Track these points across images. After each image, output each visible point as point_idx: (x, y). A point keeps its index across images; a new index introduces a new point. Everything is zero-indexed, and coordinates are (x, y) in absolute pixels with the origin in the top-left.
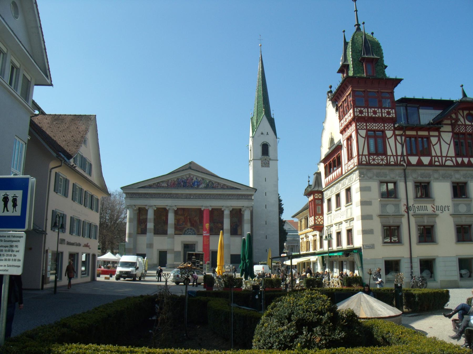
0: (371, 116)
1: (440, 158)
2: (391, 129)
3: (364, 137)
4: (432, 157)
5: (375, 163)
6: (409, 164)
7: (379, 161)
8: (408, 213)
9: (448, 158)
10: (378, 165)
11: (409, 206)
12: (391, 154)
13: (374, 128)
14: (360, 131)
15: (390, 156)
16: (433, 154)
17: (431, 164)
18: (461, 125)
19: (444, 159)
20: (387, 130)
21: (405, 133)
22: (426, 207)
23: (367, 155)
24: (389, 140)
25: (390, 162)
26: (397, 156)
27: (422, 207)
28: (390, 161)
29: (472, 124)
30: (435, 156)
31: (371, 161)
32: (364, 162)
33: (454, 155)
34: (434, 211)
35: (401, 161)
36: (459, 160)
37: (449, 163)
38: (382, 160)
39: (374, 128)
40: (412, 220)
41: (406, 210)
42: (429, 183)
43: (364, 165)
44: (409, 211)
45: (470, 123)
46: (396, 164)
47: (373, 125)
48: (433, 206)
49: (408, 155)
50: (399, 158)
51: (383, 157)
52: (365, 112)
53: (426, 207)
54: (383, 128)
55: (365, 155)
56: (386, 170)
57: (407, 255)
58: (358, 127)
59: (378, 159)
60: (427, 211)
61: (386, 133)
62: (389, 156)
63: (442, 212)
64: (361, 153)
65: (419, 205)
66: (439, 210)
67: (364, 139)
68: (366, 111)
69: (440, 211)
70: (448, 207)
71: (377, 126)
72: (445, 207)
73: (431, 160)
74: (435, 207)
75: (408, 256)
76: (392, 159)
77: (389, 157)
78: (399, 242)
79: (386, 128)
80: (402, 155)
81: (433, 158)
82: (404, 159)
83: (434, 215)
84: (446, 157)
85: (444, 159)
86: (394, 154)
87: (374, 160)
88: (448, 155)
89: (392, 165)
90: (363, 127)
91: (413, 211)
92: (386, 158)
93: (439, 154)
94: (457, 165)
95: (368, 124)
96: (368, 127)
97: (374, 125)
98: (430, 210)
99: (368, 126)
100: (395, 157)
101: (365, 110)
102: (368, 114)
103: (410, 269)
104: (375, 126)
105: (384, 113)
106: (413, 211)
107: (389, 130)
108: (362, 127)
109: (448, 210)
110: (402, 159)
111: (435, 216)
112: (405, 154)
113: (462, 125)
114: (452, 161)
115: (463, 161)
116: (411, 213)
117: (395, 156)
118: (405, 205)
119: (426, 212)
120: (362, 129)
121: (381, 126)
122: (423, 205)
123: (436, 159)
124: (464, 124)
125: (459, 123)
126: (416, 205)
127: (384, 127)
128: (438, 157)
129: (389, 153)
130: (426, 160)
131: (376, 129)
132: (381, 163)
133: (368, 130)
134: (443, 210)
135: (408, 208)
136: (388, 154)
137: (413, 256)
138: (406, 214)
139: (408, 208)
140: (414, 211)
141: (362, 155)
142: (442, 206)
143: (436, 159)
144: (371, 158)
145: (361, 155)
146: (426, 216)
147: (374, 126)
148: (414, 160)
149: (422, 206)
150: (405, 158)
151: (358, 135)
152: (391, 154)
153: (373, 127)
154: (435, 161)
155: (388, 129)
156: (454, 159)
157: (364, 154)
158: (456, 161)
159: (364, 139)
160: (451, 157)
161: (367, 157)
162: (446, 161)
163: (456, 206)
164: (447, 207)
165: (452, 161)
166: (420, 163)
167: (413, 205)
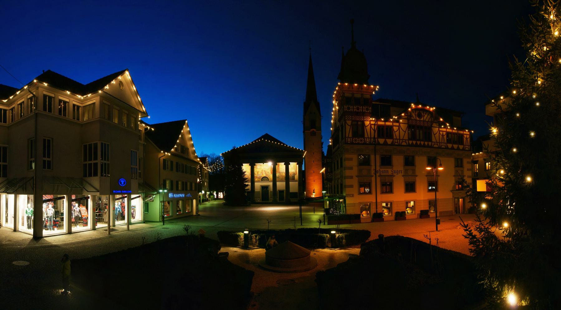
1: (398, 140)
3: (350, 125)
6: (379, 144)
7: (359, 141)
8: (376, 175)
9: (403, 141)
10: (358, 144)
15: (366, 138)
16: (395, 137)
17: (392, 144)
18: (413, 120)
19: (401, 141)
20: (365, 121)
21: (377, 123)
23: (351, 137)
25: (366, 142)
26: (371, 138)
30: (395, 139)
31: (354, 141)
32: (349, 142)
33: (407, 139)
35: (373, 142)
36: (410, 142)
37: (404, 144)
39: (357, 119)
43: (349, 144)
45: (419, 119)
46: (370, 144)
49: (377, 138)
50: (372, 139)
51: (362, 139)
54: (363, 119)
55: (350, 138)
58: (346, 119)
62: (366, 138)
64: (347, 136)
65: (383, 170)
67: (350, 127)
68: (352, 108)
73: (393, 142)
74: (393, 171)
75: (375, 201)
76: (368, 140)
77: (365, 139)
78: (370, 192)
79: (365, 119)
81: (394, 140)
82: (375, 140)
83: (392, 176)
84: (403, 140)
85: (401, 141)
86: (369, 137)
87: (356, 140)
88: (404, 139)
89: (368, 144)
93: (398, 138)
94: (409, 145)
97: (357, 117)
98: (390, 173)
100: (370, 139)
101: (352, 107)
103: (376, 209)
105: (364, 109)
109: (401, 173)
110: (374, 140)
112: (376, 137)
113: (414, 120)
114: (406, 142)
115: (412, 143)
116: (378, 174)
119: (388, 174)
120: (349, 120)
123: (396, 141)
124: (415, 118)
126: (381, 170)
128: (397, 139)
129: (366, 136)
130: (389, 141)
132: (360, 142)
133: (353, 121)
135: (376, 172)
136: (365, 137)
138: (374, 175)
141: (348, 137)
143: (396, 141)
144: (354, 140)
148: (381, 141)
150: (376, 139)
151: (346, 124)
153: (356, 119)
156: (407, 141)
157: (349, 137)
158: (408, 142)
159: (350, 127)
160: (406, 140)
162: (402, 142)
165: (406, 142)
166: (385, 144)
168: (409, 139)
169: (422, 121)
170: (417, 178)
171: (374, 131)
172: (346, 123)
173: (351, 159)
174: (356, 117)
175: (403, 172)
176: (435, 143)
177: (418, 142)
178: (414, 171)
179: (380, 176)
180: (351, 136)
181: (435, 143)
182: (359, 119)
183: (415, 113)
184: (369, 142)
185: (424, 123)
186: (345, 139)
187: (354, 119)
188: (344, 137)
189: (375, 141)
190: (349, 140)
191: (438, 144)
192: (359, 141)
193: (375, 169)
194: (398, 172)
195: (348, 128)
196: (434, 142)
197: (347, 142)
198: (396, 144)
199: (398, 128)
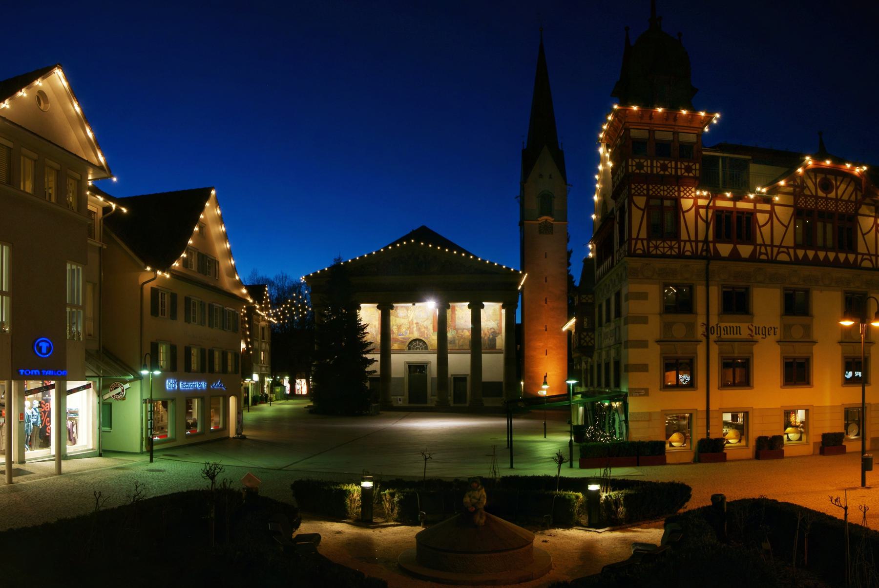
0: (658, 173)
1: (769, 249)
2: (690, 196)
4: (756, 245)
5: (659, 252)
6: (717, 256)
8: (707, 337)
9: (782, 249)
10: (664, 256)
11: (710, 327)
12: (687, 239)
13: (662, 193)
14: (634, 198)
15: (685, 241)
16: (759, 241)
17: (753, 258)
19: (775, 250)
20: (683, 197)
21: (714, 203)
22: (738, 328)
23: (645, 239)
24: (685, 214)
25: (684, 252)
26: (697, 241)
27: (732, 328)
28: (685, 250)
29: (827, 196)
30: (761, 245)
31: (651, 249)
33: (792, 245)
34: (751, 336)
35: (702, 250)
36: (801, 253)
37: (783, 257)
38: (671, 248)
39: (662, 193)
40: (715, 350)
41: (706, 334)
42: (747, 289)
43: (639, 256)
44: (710, 334)
45: (824, 195)
46: (694, 256)
47: (659, 188)
48: (751, 327)
49: (714, 242)
50: (700, 245)
51: (673, 243)
53: (738, 328)
54: (676, 194)
55: (642, 240)
56: (677, 264)
57: (703, 408)
58: (633, 191)
59: (664, 247)
60: (740, 334)
61: (680, 202)
62: (682, 241)
63: (764, 336)
64: (634, 236)
65: (728, 325)
66: (759, 334)
68: (649, 165)
69: (761, 336)
70: (774, 330)
71: (666, 191)
72: (770, 329)
75: (704, 408)
76: (688, 247)
77: (682, 244)
78: (691, 385)
79: (682, 194)
80: (706, 241)
81: (758, 247)
82: (708, 246)
83: (752, 341)
84: (780, 246)
85: (775, 250)
86: (693, 238)
87: (656, 247)
88: (783, 245)
90: (642, 192)
91: (717, 334)
93: (768, 242)
94: (797, 261)
95: (651, 187)
96: (651, 192)
98: (745, 334)
99: (651, 190)
100: (693, 244)
103: (705, 428)
104: (664, 190)
105: (681, 169)
106: (717, 334)
108: (639, 191)
109: (775, 334)
110: (705, 248)
111: (753, 343)
112: (711, 238)
113: (812, 196)
114: (788, 254)
115: (806, 255)
116: (713, 337)
118: (705, 325)
120: (639, 195)
121: (673, 191)
122: (734, 325)
123: (763, 250)
124: (814, 194)
125: (807, 192)
126: (723, 325)
128: (766, 246)
129: (684, 236)
130: (745, 250)
132: (669, 253)
133: (649, 198)
134: (765, 334)
135: (708, 330)
136: (682, 239)
137: (711, 408)
138: (704, 339)
139: (707, 329)
140: (719, 335)
141: (637, 239)
142: (765, 328)
143: (763, 250)
144: (651, 245)
145: (634, 239)
146: (736, 343)
147: (661, 190)
148: (725, 249)
149: (733, 327)
150: (711, 245)
151: (633, 205)
153: (659, 192)
154: (761, 253)
156: (791, 251)
157: (640, 237)
158: (795, 254)
159: (641, 212)
160: (787, 248)
161: (645, 242)
162: (778, 253)
163: (787, 328)
164: (773, 329)
165: (788, 254)
166: (735, 256)
167: (717, 325)
168: (797, 246)
169: (832, 199)
170: (816, 349)
171: (704, 224)
172: (631, 201)
173: (643, 296)
174: (659, 188)
175: (778, 331)
176: (865, 257)
177: (822, 255)
178: (808, 329)
179: (718, 341)
180: (643, 234)
181: (865, 257)
182: (666, 193)
183: (814, 180)
184: (692, 252)
185: (837, 206)
186: (630, 244)
187: (654, 192)
188: (626, 237)
189: (708, 250)
190: (639, 245)
191: (874, 258)
192: (666, 250)
193: (705, 322)
194: (765, 332)
195: (637, 215)
196: (863, 254)
197: (635, 250)
198: (763, 257)
199: (767, 215)
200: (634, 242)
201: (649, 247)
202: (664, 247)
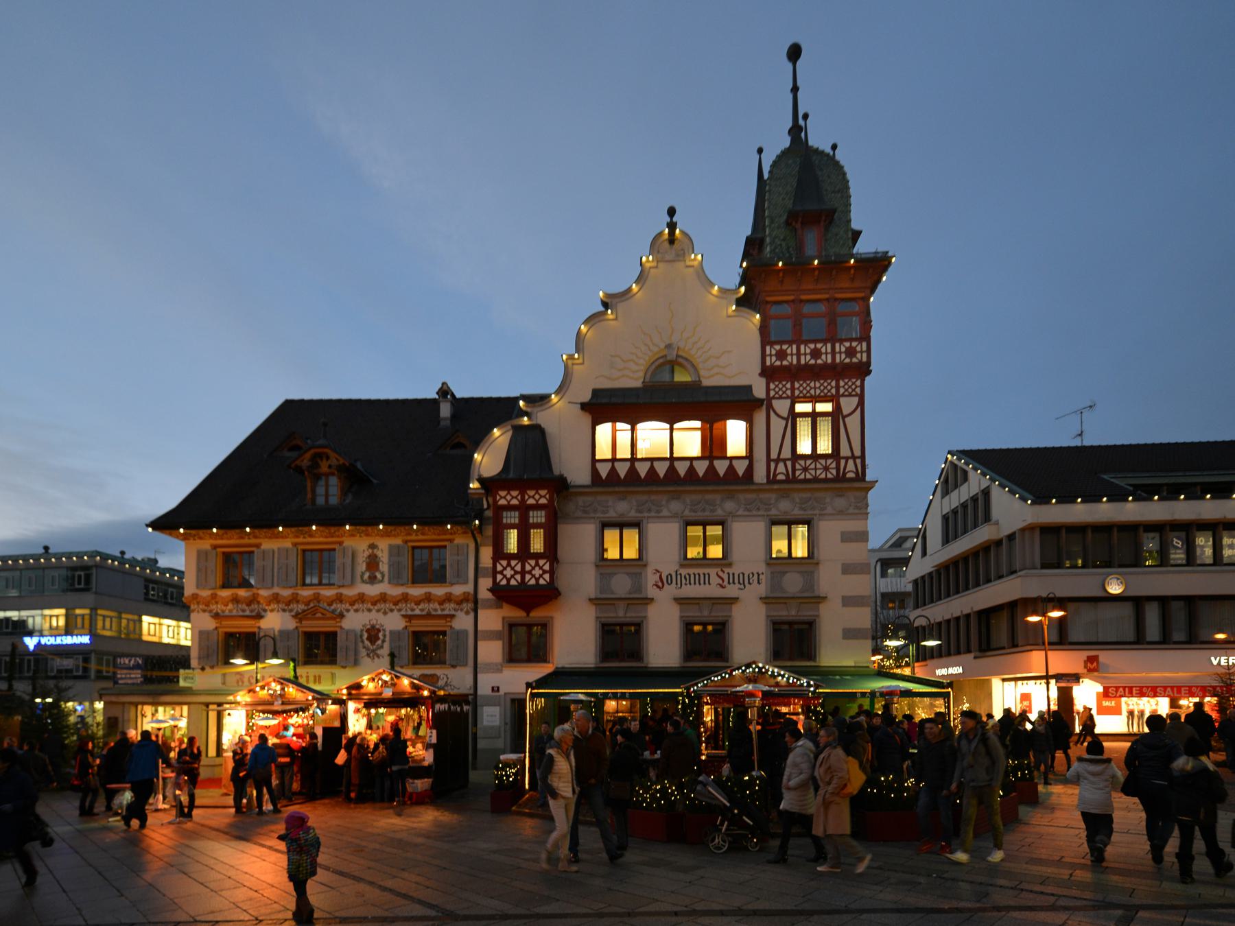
0: (806, 364)
2: (854, 393)
5: (808, 476)
10: (816, 480)
12: (849, 454)
14: (775, 402)
15: (847, 459)
20: (843, 395)
23: (788, 459)
24: (846, 419)
31: (798, 473)
38: (826, 469)
52: (792, 355)
54: (833, 391)
55: (785, 461)
62: (843, 458)
64: (774, 455)
67: (784, 422)
77: (843, 462)
79: (842, 391)
86: (858, 453)
87: (805, 469)
92: (834, 463)
97: (812, 384)
102: (799, 360)
107: (850, 395)
117: (858, 457)
120: (781, 398)
121: (829, 387)
127: (838, 387)
129: (845, 451)
131: (817, 393)
132: (823, 476)
141: (778, 460)
144: (798, 466)
145: (773, 460)
151: (772, 414)
152: (849, 454)
155: (846, 393)
157: (782, 456)
159: (784, 422)
161: (789, 464)
192: (813, 466)
200: (773, 465)
201: (794, 470)
202: (816, 469)
